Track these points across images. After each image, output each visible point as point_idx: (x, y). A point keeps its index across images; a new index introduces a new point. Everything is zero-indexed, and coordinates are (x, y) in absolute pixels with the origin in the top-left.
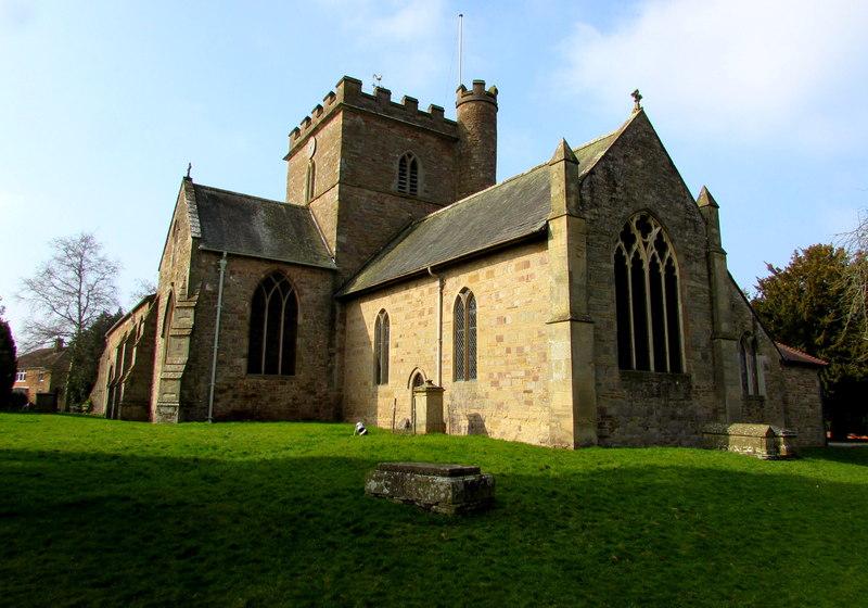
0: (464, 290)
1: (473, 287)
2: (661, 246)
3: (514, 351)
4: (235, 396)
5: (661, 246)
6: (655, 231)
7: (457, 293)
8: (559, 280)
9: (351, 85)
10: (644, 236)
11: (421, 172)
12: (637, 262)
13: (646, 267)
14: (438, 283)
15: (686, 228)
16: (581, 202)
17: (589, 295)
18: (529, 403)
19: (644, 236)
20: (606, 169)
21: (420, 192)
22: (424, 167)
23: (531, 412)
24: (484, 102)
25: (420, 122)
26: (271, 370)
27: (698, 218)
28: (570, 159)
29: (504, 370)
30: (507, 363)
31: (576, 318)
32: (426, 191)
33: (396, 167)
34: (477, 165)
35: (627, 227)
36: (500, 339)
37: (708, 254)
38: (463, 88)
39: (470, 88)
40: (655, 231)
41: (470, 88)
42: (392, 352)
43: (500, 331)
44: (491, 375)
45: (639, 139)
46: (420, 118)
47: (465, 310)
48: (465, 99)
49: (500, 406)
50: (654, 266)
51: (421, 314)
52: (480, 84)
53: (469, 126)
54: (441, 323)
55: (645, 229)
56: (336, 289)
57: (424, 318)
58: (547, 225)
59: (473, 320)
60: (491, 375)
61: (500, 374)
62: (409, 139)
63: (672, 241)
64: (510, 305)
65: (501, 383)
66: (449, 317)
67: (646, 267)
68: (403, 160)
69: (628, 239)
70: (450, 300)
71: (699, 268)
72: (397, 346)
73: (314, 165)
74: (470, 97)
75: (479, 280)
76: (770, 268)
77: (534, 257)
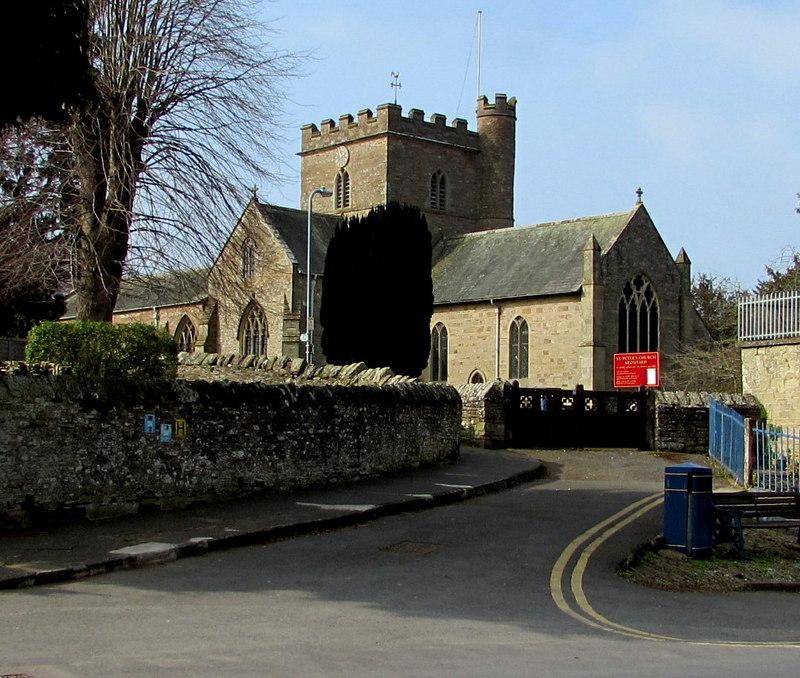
0: (518, 318)
1: (524, 317)
2: (649, 294)
3: (555, 361)
5: (649, 294)
6: (645, 285)
8: (587, 322)
9: (394, 109)
10: (638, 289)
11: (449, 187)
12: (633, 306)
13: (638, 309)
14: (497, 310)
15: (666, 281)
16: (602, 273)
17: (604, 330)
19: (638, 289)
20: (618, 250)
21: (448, 208)
22: (451, 182)
24: (504, 112)
25: (447, 138)
27: (675, 272)
28: (597, 249)
30: (550, 368)
31: (596, 345)
32: (452, 206)
33: (429, 184)
34: (498, 180)
35: (628, 284)
36: (546, 353)
37: (680, 297)
38: (485, 100)
39: (492, 101)
40: (645, 285)
41: (492, 101)
42: (450, 357)
44: (539, 375)
45: (641, 226)
46: (447, 134)
47: (519, 334)
48: (487, 112)
50: (643, 308)
51: (481, 330)
52: (501, 98)
53: (492, 138)
55: (639, 284)
58: (581, 288)
59: (525, 339)
60: (539, 375)
61: (545, 375)
63: (656, 291)
66: (506, 335)
67: (638, 309)
68: (434, 177)
69: (628, 292)
70: (507, 322)
71: (674, 307)
72: (456, 352)
73: (346, 175)
74: (492, 111)
75: (532, 314)
76: (770, 272)
77: (571, 304)
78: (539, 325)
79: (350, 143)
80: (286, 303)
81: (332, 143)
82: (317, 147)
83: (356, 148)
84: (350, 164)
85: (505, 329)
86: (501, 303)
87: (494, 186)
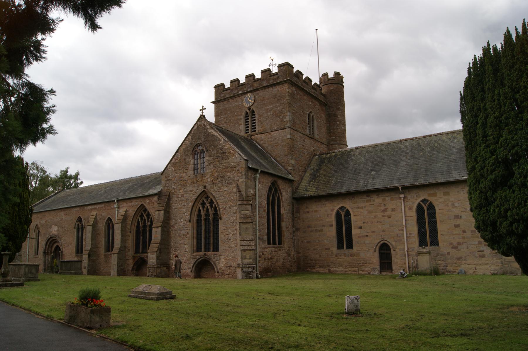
1: (431, 199)
4: (265, 260)
7: (419, 200)
18: (483, 256)
23: (483, 260)
26: (274, 243)
29: (461, 241)
36: (457, 226)
39: (331, 75)
42: (355, 232)
43: (458, 222)
49: (459, 259)
51: (385, 211)
54: (405, 217)
56: (294, 193)
57: (386, 214)
62: (311, 103)
64: (464, 210)
65: (460, 248)
72: (361, 228)
78: (447, 205)
79: (257, 90)
80: (239, 191)
81: (240, 92)
82: (227, 96)
83: (261, 93)
84: (256, 104)
85: (410, 209)
86: (407, 189)
87: (338, 125)
